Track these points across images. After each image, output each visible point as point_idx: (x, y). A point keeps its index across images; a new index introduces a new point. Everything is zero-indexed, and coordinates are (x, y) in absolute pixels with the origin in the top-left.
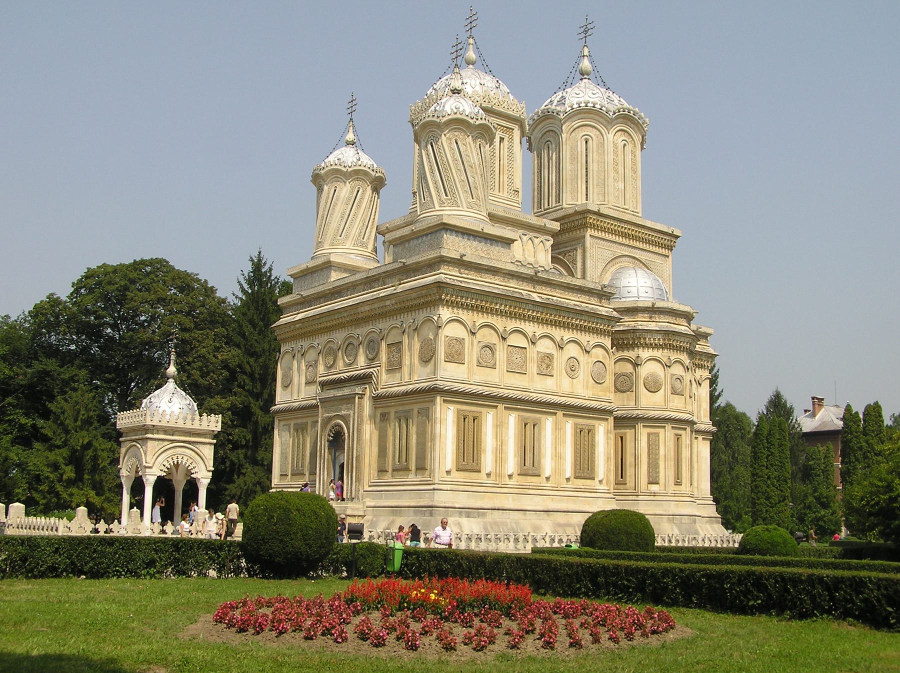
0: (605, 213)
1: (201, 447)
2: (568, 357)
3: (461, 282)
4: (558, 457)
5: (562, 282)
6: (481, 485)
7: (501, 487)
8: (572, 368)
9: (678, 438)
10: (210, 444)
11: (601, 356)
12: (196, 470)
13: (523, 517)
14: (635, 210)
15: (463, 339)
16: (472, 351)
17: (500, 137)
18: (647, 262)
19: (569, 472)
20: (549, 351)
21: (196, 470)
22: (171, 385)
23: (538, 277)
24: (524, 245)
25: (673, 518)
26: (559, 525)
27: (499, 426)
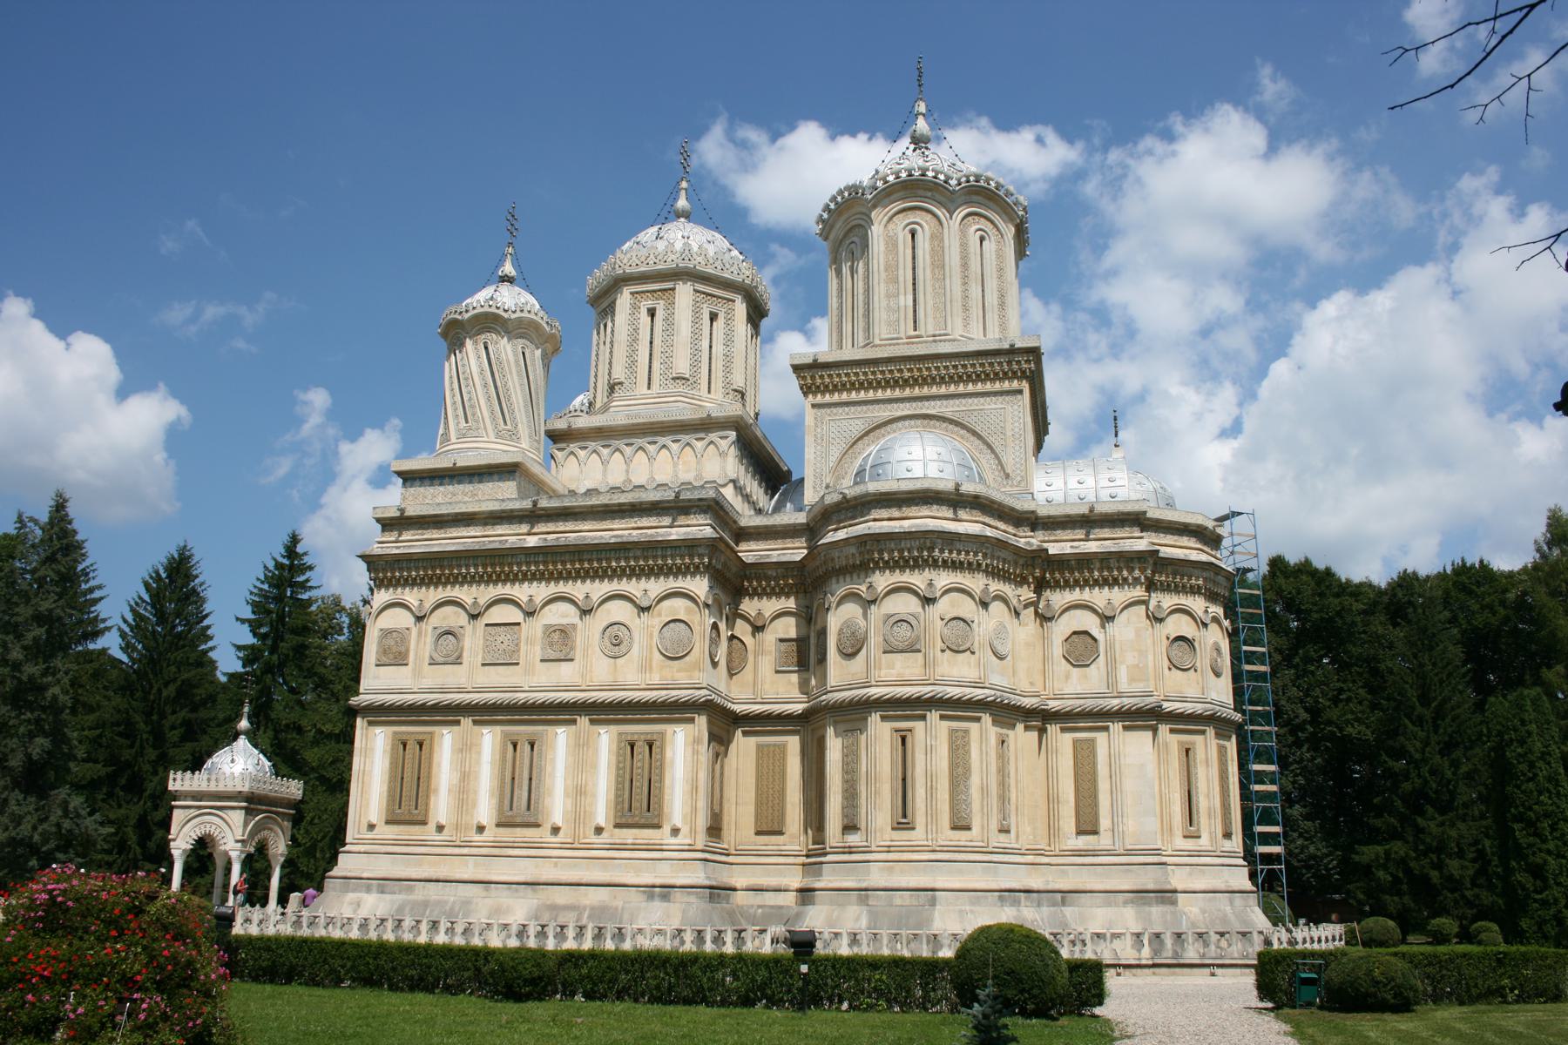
0: (830, 360)
1: (231, 812)
2: (605, 624)
3: (398, 548)
4: (579, 792)
5: (592, 506)
6: (423, 843)
7: (460, 846)
8: (616, 640)
9: (904, 739)
10: (241, 808)
11: (682, 612)
12: (225, 841)
13: (484, 894)
14: (937, 332)
15: (408, 629)
16: (421, 644)
17: (649, 310)
18: (957, 414)
19: (602, 812)
20: (564, 621)
21: (225, 841)
22: (242, 742)
23: (543, 509)
24: (675, 459)
25: (867, 896)
26: (554, 908)
27: (466, 749)
